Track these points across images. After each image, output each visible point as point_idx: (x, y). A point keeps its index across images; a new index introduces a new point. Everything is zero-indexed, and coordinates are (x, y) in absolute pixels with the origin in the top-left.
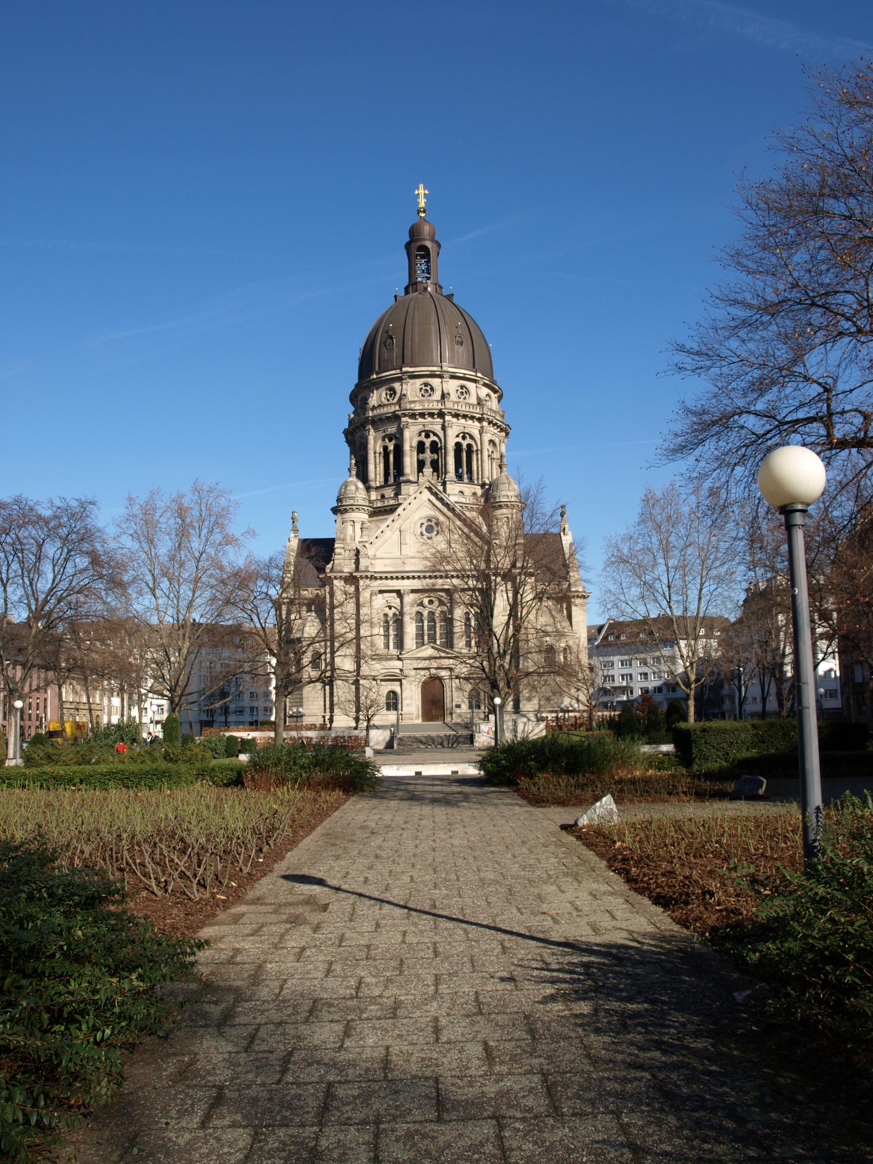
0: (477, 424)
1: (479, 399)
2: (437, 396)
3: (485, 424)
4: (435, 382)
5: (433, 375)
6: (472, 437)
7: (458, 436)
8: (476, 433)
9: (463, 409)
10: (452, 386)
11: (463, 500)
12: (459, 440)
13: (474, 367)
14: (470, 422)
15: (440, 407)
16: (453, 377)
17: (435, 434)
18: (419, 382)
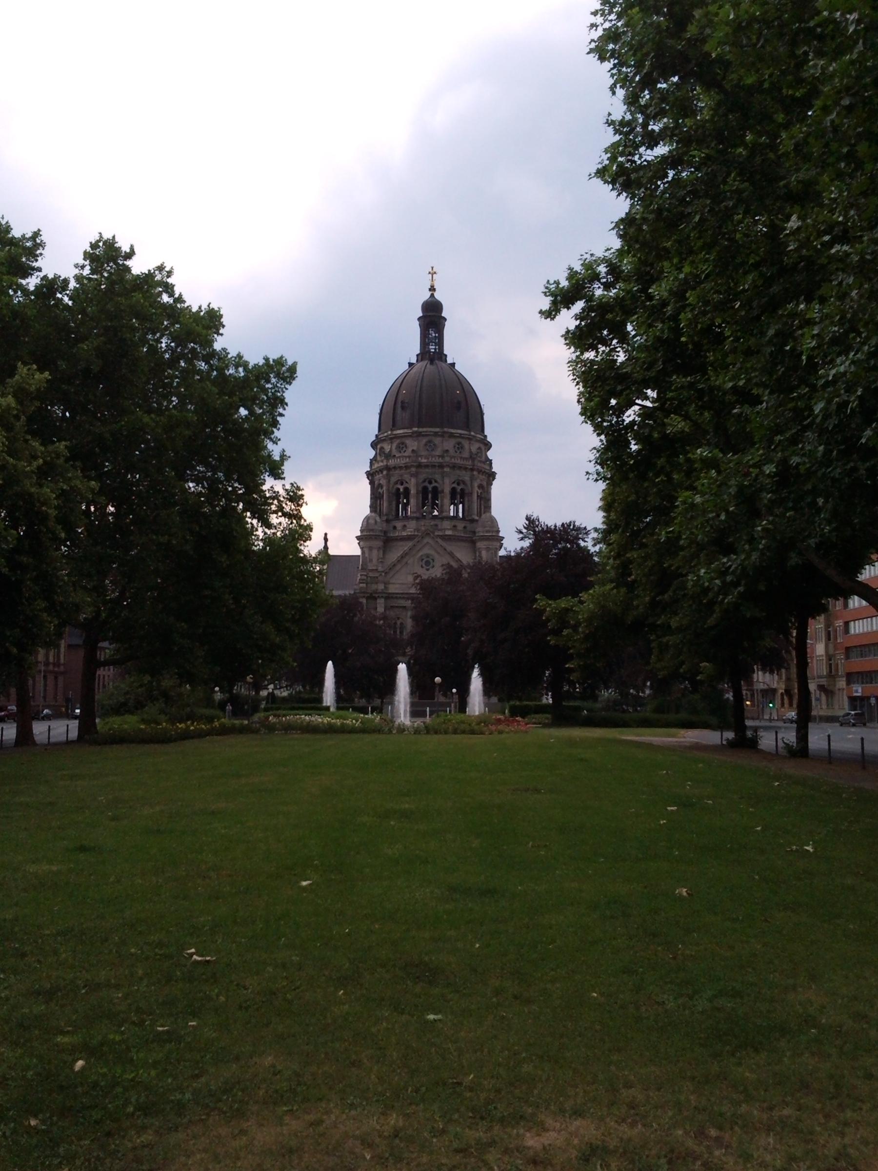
0: (469, 473)
1: (471, 452)
2: (438, 452)
3: (475, 473)
4: (437, 440)
5: (436, 434)
6: (464, 483)
8: (467, 479)
9: (459, 461)
10: (449, 444)
11: (457, 534)
12: (455, 485)
13: (468, 427)
14: (464, 472)
15: (441, 460)
16: (452, 436)
17: (436, 481)
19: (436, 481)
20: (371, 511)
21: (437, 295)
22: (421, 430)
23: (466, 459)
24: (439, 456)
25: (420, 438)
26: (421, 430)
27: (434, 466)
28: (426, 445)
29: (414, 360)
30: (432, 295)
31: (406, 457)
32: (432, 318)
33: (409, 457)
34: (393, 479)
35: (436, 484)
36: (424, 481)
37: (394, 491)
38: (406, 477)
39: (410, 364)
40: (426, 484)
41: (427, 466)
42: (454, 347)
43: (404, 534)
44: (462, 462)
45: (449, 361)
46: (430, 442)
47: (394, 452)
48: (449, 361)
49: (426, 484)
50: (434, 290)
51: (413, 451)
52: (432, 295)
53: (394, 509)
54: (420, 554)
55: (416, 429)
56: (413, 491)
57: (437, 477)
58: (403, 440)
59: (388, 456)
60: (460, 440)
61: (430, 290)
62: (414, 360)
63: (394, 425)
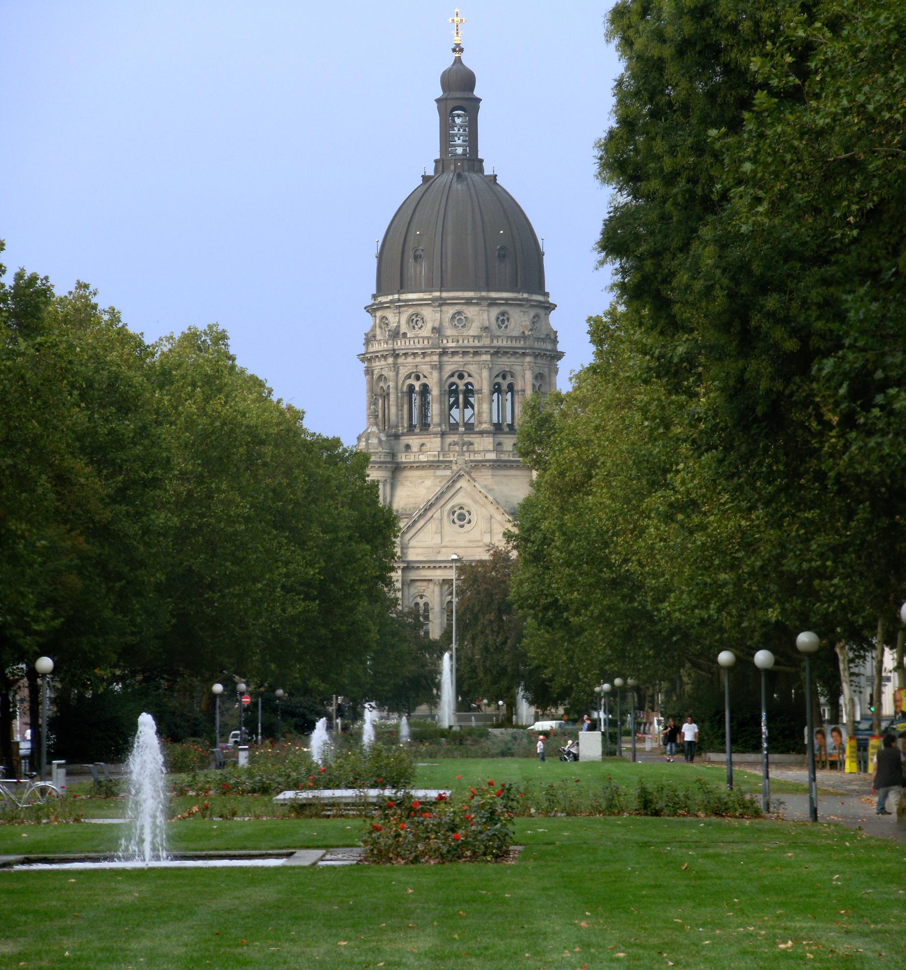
2: (473, 331)
5: (469, 302)
7: (497, 376)
14: (513, 359)
15: (476, 343)
18: (450, 311)
19: (470, 376)
20: (371, 425)
21: (468, 61)
22: (445, 295)
23: (516, 338)
24: (474, 337)
25: (444, 308)
26: (445, 295)
27: (465, 353)
28: (453, 318)
29: (431, 172)
30: (458, 61)
31: (423, 338)
32: (459, 95)
33: (428, 338)
34: (403, 372)
35: (470, 380)
36: (452, 375)
37: (405, 389)
38: (425, 369)
39: (426, 179)
40: (455, 379)
41: (454, 353)
42: (493, 155)
43: (423, 458)
44: (509, 344)
45: (488, 171)
46: (459, 313)
47: (404, 328)
48: (488, 171)
49: (455, 379)
50: (461, 50)
51: (434, 328)
52: (458, 61)
53: (406, 416)
54: (449, 506)
55: (437, 294)
56: (435, 392)
57: (472, 368)
58: (419, 309)
59: (396, 334)
60: (503, 308)
61: (454, 50)
62: (431, 172)
63: (402, 287)
